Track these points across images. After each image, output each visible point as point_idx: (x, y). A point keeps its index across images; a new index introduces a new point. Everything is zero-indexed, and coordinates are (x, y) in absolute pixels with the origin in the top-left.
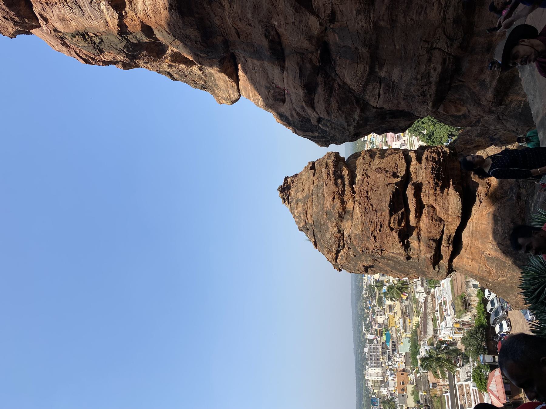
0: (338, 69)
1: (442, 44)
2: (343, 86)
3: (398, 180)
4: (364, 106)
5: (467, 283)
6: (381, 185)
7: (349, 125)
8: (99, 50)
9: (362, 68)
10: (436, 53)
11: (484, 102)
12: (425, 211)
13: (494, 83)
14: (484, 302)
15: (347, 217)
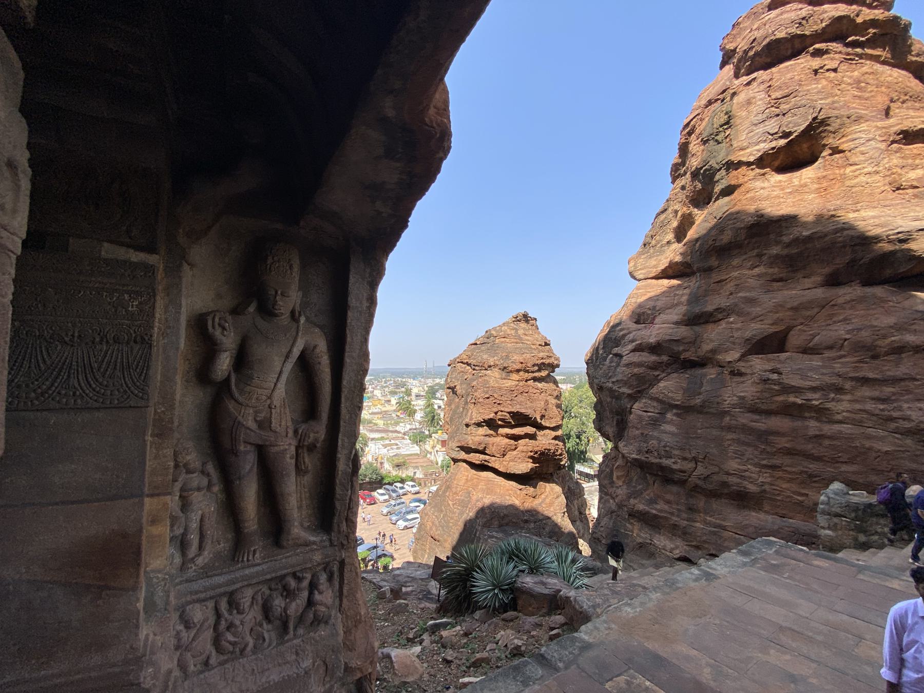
0: (675, 375)
1: (701, 470)
2: (657, 380)
3: (539, 420)
4: (634, 398)
5: (417, 467)
6: (534, 405)
7: (613, 382)
8: (708, 140)
9: (678, 398)
10: (692, 465)
11: (632, 501)
12: (512, 442)
13: (654, 512)
14: (402, 481)
15: (504, 374)
